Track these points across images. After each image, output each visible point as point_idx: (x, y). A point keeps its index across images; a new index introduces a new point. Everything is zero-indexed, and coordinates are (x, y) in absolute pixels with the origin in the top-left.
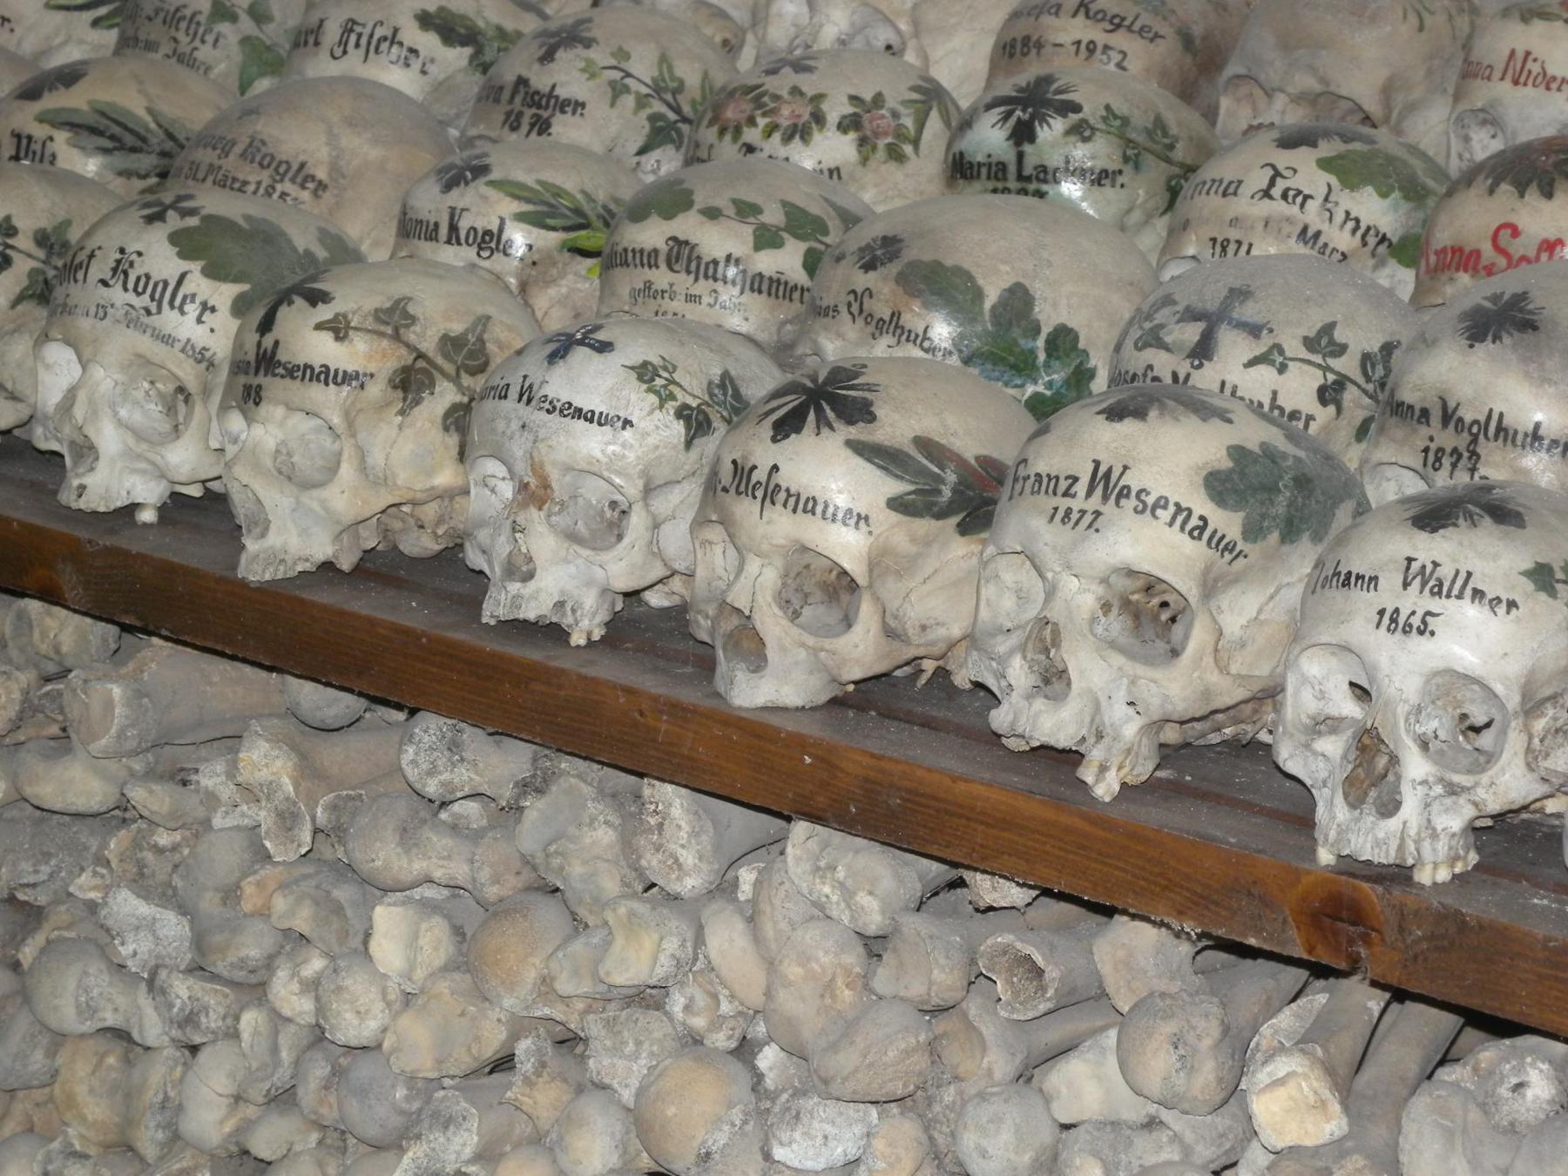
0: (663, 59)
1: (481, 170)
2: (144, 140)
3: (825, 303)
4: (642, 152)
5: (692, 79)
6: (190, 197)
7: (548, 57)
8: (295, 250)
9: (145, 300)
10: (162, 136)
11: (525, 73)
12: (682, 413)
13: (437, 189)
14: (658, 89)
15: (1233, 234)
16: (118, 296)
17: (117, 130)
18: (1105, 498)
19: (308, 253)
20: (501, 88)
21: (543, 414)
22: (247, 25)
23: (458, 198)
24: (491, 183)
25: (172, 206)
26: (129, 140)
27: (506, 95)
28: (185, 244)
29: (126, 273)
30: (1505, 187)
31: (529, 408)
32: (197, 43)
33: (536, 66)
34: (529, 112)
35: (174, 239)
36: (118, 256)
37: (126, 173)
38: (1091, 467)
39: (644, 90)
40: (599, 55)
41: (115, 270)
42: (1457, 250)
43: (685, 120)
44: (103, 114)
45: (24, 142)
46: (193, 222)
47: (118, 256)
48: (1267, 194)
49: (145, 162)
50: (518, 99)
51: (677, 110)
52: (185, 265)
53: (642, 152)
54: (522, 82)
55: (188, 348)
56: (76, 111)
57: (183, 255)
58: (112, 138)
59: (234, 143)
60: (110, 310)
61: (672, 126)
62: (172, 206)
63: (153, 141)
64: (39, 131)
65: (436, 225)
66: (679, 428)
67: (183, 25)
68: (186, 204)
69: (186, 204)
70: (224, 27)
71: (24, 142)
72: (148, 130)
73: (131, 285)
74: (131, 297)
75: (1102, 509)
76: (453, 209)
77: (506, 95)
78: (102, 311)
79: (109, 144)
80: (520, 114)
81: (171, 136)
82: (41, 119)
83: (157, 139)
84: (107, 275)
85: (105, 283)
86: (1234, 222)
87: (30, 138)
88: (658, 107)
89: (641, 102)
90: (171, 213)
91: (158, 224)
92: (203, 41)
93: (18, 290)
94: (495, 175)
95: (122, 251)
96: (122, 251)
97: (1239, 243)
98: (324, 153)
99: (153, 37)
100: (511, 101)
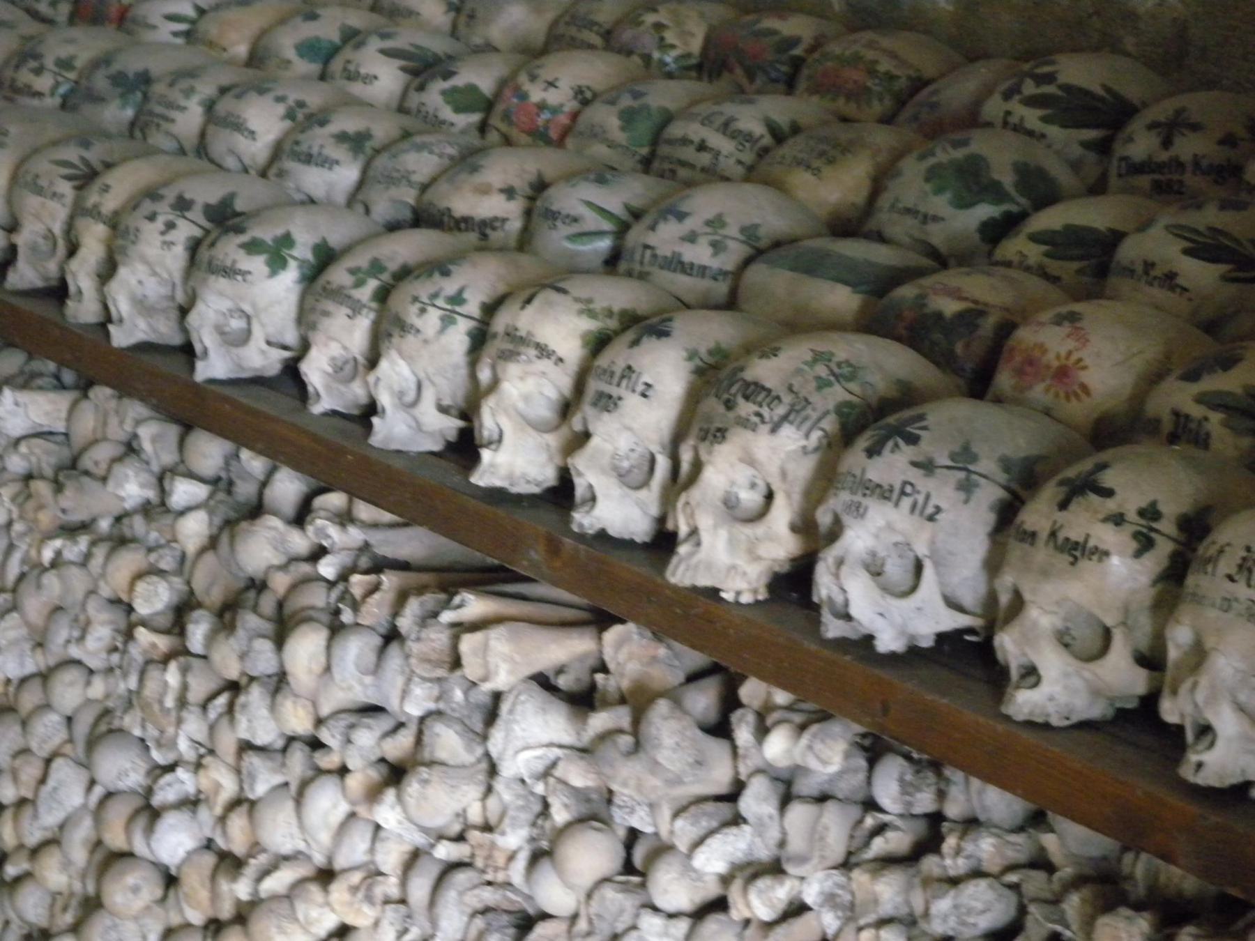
45: (1182, 420)
56: (1229, 394)
64: (1196, 411)
71: (1182, 420)
82: (1201, 399)
87: (1187, 417)
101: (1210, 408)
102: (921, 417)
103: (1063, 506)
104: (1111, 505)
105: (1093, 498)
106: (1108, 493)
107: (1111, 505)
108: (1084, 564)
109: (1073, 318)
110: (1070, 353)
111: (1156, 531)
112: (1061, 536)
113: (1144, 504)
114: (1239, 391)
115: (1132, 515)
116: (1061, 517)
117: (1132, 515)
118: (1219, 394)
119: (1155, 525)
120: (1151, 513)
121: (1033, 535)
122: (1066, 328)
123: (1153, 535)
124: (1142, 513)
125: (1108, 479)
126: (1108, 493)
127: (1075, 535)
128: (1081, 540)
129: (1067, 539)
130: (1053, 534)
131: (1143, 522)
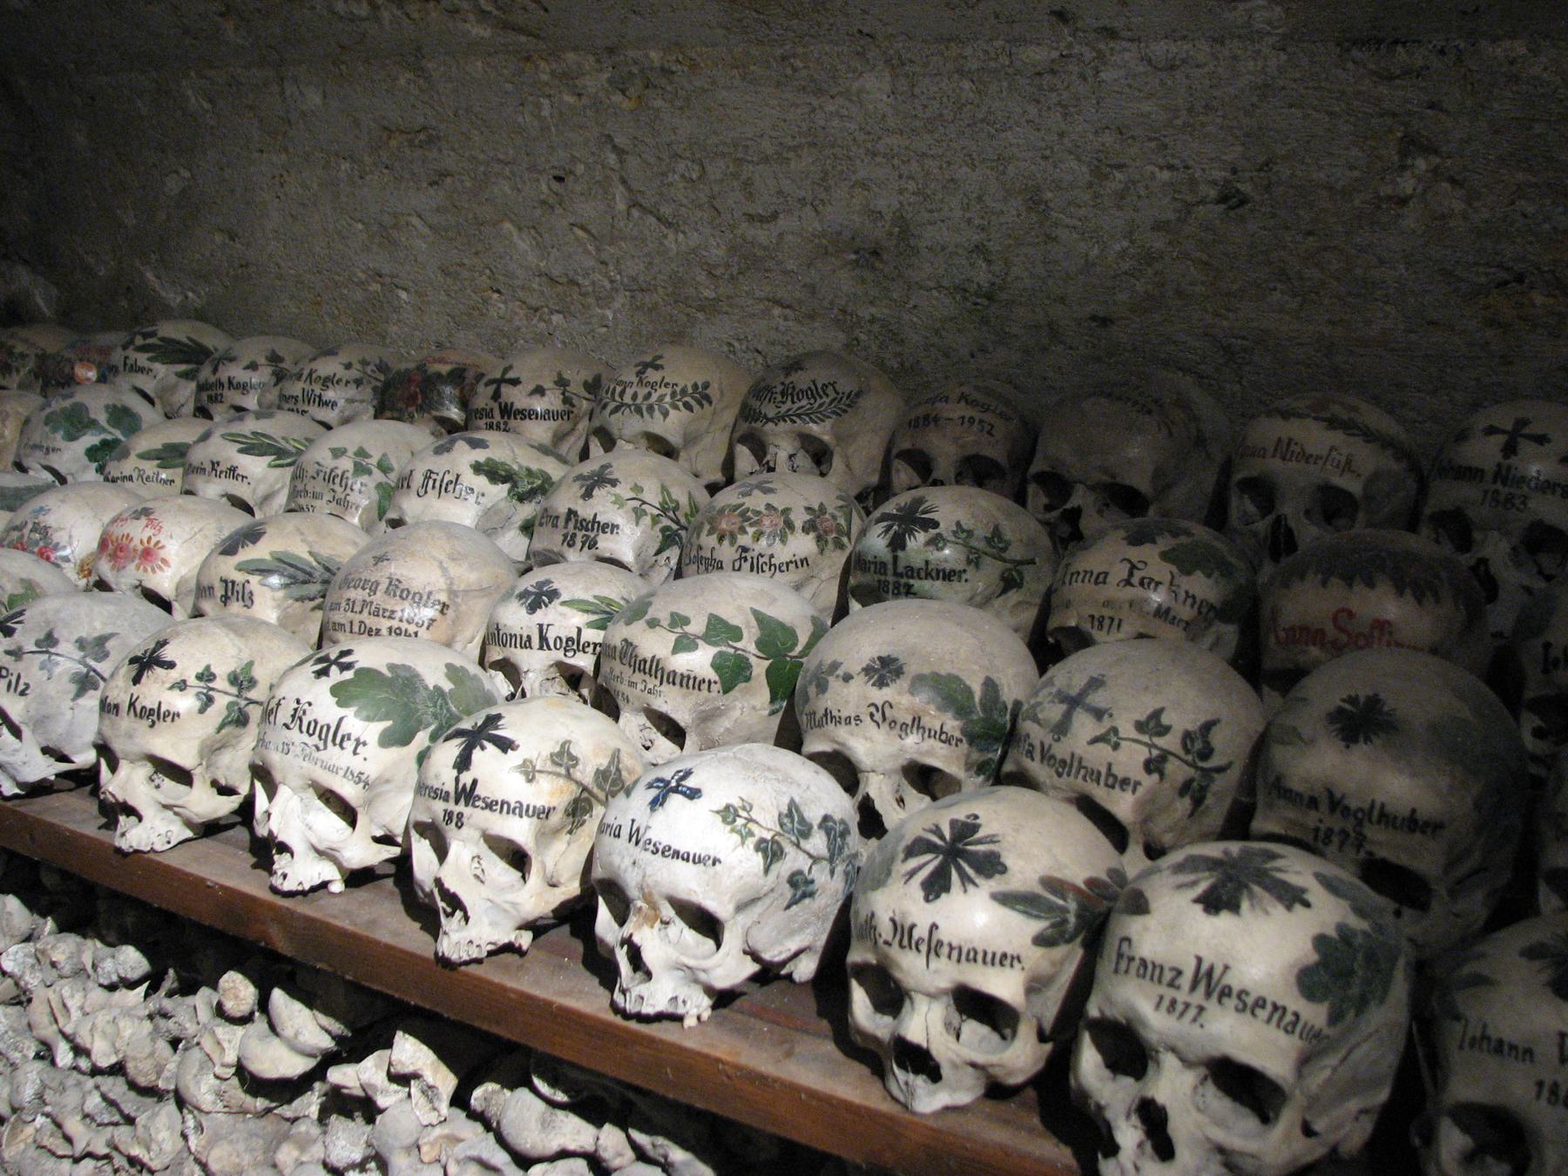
0: (664, 489)
1: (553, 595)
2: (310, 574)
3: (844, 714)
4: (658, 553)
5: (684, 501)
6: (349, 652)
7: (588, 495)
8: (426, 688)
11: (573, 507)
12: (761, 846)
13: (524, 611)
14: (664, 510)
15: (1107, 612)
16: (295, 735)
17: (292, 570)
18: (1208, 994)
19: (437, 688)
21: (648, 854)
22: (378, 476)
23: (541, 616)
24: (564, 603)
25: (335, 662)
26: (301, 576)
27: (561, 522)
28: (341, 694)
30: (1334, 580)
31: (638, 849)
33: (581, 501)
34: (580, 534)
35: (336, 690)
37: (301, 599)
38: (1193, 962)
39: (656, 512)
40: (623, 490)
41: (293, 716)
42: (1304, 629)
43: (683, 528)
44: (280, 560)
46: (349, 675)
48: (1128, 582)
49: (314, 589)
50: (571, 525)
51: (677, 522)
52: (342, 712)
53: (658, 553)
54: (571, 513)
55: (348, 772)
56: (262, 561)
57: (339, 704)
58: (290, 577)
59: (378, 584)
61: (676, 533)
62: (335, 662)
63: (317, 574)
64: (239, 577)
65: (529, 637)
66: (758, 859)
67: (337, 481)
68: (344, 660)
69: (344, 660)
70: (365, 478)
73: (304, 728)
74: (305, 737)
75: (1204, 1004)
77: (561, 522)
78: (286, 749)
80: (574, 535)
81: (327, 569)
82: (240, 568)
83: (319, 573)
85: (287, 726)
86: (1107, 604)
87: (233, 582)
88: (665, 522)
89: (655, 520)
90: (334, 669)
91: (324, 678)
93: (220, 720)
94: (565, 597)
95: (298, 702)
96: (298, 702)
97: (1112, 619)
98: (442, 583)
99: (318, 490)
102: (21, 613)
103: (136, 680)
104: (174, 675)
105: (158, 670)
106: (171, 665)
107: (174, 675)
108: (160, 725)
109: (146, 512)
110: (149, 539)
113: (200, 670)
114: (268, 557)
115: (192, 681)
116: (135, 690)
117: (192, 681)
118: (253, 561)
120: (206, 676)
121: (117, 707)
122: (144, 521)
124: (200, 677)
126: (171, 665)
127: (150, 704)
129: (143, 708)
130: (132, 705)
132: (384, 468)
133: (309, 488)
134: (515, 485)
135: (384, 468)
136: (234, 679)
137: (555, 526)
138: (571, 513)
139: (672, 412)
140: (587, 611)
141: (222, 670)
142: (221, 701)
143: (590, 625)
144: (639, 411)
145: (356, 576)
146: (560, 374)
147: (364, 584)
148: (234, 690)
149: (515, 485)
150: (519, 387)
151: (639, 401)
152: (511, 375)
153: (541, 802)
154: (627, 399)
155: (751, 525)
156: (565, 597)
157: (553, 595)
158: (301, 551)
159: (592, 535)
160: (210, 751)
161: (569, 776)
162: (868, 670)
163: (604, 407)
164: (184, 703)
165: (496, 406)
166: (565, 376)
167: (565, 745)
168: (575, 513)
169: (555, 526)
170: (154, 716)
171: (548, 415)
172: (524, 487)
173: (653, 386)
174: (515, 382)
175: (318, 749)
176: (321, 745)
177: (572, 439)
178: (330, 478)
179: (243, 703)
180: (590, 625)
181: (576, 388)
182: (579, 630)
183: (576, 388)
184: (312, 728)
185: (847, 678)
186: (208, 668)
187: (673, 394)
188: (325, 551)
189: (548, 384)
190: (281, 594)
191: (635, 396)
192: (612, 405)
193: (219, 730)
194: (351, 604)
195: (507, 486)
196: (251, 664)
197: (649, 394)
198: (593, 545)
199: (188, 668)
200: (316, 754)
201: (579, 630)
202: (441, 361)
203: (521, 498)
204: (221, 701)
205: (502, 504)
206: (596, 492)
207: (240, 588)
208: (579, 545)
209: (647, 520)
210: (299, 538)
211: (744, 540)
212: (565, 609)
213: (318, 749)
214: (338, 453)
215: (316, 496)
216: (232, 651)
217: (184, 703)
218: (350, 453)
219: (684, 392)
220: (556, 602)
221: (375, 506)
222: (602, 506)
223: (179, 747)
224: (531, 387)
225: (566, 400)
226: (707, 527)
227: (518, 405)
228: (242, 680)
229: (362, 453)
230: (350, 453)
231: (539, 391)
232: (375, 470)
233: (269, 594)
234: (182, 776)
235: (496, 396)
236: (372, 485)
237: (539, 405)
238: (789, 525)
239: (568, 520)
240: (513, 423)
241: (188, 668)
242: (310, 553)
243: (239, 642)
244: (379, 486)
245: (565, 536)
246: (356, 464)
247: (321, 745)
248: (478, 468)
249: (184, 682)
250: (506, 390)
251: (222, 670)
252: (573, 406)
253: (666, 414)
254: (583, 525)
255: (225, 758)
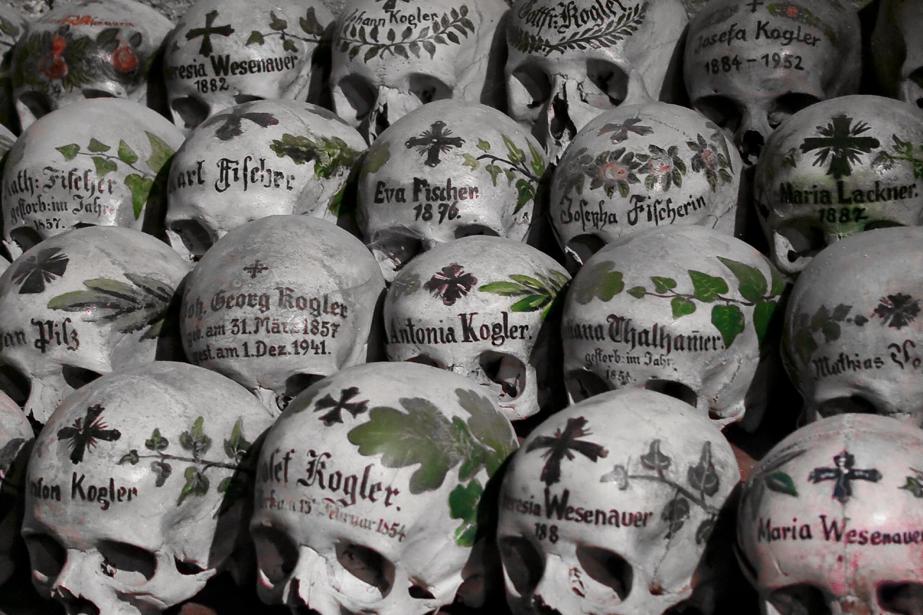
2: (133, 300)
7: (433, 160)
9: (340, 493)
10: (144, 293)
11: (419, 176)
16: (315, 492)
17: (114, 299)
20: (402, 190)
26: (125, 304)
27: (409, 195)
29: (320, 473)
32: (97, 194)
34: (435, 205)
35: (355, 436)
36: (311, 459)
40: (470, 148)
41: (310, 471)
43: (533, 179)
44: (97, 289)
47: (311, 459)
50: (422, 196)
58: (114, 306)
60: (313, 505)
63: (139, 298)
64: (57, 316)
67: (81, 184)
68: (351, 401)
70: (111, 176)
72: (134, 292)
73: (326, 483)
76: (463, 316)
77: (409, 195)
79: (111, 312)
81: (149, 291)
82: (54, 305)
84: (305, 476)
85: (303, 482)
87: (50, 323)
90: (344, 412)
92: (101, 191)
93: (180, 490)
95: (313, 454)
99: (57, 199)
100: (416, 199)
101: (66, 310)
103: (77, 457)
104: (121, 446)
106: (114, 435)
107: (121, 446)
108: (115, 506)
111: (167, 457)
112: (85, 486)
113: (149, 437)
115: (143, 450)
117: (143, 450)
119: (164, 452)
120: (157, 442)
123: (166, 461)
124: (150, 445)
125: (107, 420)
126: (114, 435)
128: (107, 485)
129: (92, 488)
131: (155, 453)
132: (129, 159)
133: (46, 199)
134: (318, 161)
135: (129, 159)
136: (187, 442)
137: (401, 199)
138: (419, 183)
139: (439, 47)
140: (508, 294)
141: (172, 433)
142: (179, 469)
143: (516, 308)
144: (400, 50)
145: (236, 293)
146: (273, 15)
147: (250, 300)
148: (189, 455)
149: (318, 161)
150: (232, 36)
151: (398, 39)
152: (217, 23)
153: (636, 508)
154: (383, 39)
155: (641, 171)
156: (481, 282)
157: (469, 281)
158: (116, 275)
159: (450, 203)
160: (173, 522)
161: (662, 479)
162: (881, 311)
163: (355, 51)
164: (138, 476)
165: (207, 62)
166: (280, 16)
167: (655, 445)
168: (425, 182)
169: (401, 199)
170: (108, 496)
171: (270, 65)
172: (327, 161)
173: (410, 20)
174: (226, 31)
175: (345, 504)
176: (348, 499)
177: (296, 89)
178: (71, 182)
179: (201, 467)
180: (516, 308)
181: (294, 29)
182: (505, 315)
183: (294, 29)
184: (336, 481)
185: (861, 321)
186: (156, 432)
187: (436, 27)
188: (140, 271)
189: (265, 30)
190: (108, 327)
191: (391, 35)
192: (365, 49)
193: (179, 504)
194: (240, 326)
195: (312, 162)
196: (200, 420)
197: (409, 30)
198: (453, 214)
199: (135, 437)
200: (343, 510)
201: (505, 315)
202: (87, 20)
203: (327, 173)
204: (179, 469)
205: (312, 184)
206: (441, 155)
207: (60, 329)
208: (437, 216)
209: (503, 177)
210: (107, 260)
211: (637, 189)
212: (486, 295)
213: (345, 504)
214: (70, 151)
215: (57, 207)
216: (177, 409)
217: (138, 476)
218: (84, 148)
219: (445, 21)
220: (475, 288)
221: (131, 204)
222: (453, 169)
223: (137, 528)
224: (246, 35)
225: (288, 45)
226: (588, 181)
227: (235, 58)
228: (194, 442)
229: (96, 146)
230: (84, 148)
231: (257, 38)
232: (120, 163)
233: (94, 329)
234: (143, 560)
235: (206, 49)
236: (120, 181)
237: (256, 53)
238: (679, 164)
239: (416, 191)
240: (231, 79)
241: (135, 437)
242: (127, 275)
243: (180, 396)
244: (128, 180)
245: (418, 209)
246: (97, 161)
247: (348, 499)
248: (279, 148)
249: (134, 452)
250: (216, 41)
251: (172, 433)
252: (295, 50)
253: (432, 50)
254: (435, 193)
255: (185, 531)
